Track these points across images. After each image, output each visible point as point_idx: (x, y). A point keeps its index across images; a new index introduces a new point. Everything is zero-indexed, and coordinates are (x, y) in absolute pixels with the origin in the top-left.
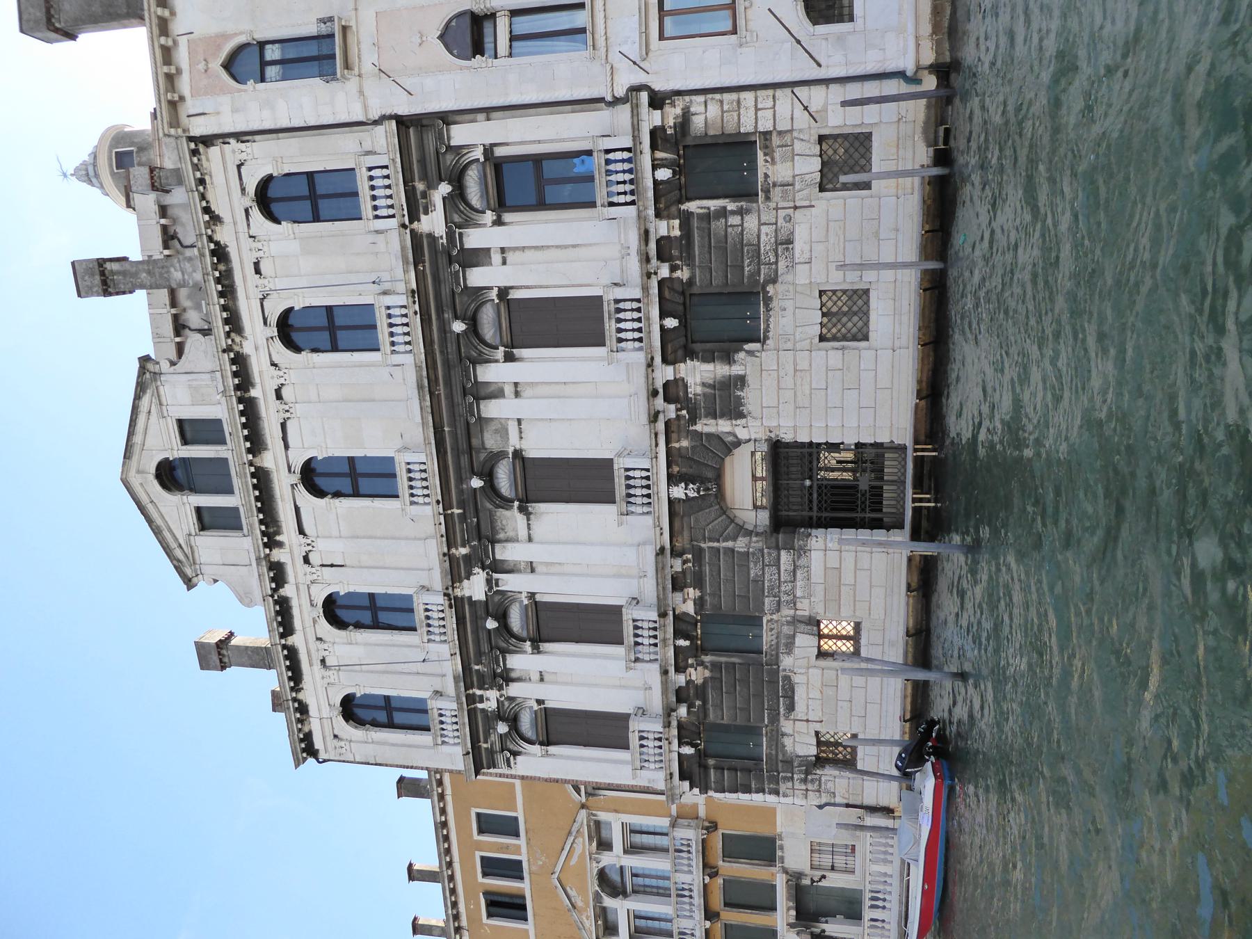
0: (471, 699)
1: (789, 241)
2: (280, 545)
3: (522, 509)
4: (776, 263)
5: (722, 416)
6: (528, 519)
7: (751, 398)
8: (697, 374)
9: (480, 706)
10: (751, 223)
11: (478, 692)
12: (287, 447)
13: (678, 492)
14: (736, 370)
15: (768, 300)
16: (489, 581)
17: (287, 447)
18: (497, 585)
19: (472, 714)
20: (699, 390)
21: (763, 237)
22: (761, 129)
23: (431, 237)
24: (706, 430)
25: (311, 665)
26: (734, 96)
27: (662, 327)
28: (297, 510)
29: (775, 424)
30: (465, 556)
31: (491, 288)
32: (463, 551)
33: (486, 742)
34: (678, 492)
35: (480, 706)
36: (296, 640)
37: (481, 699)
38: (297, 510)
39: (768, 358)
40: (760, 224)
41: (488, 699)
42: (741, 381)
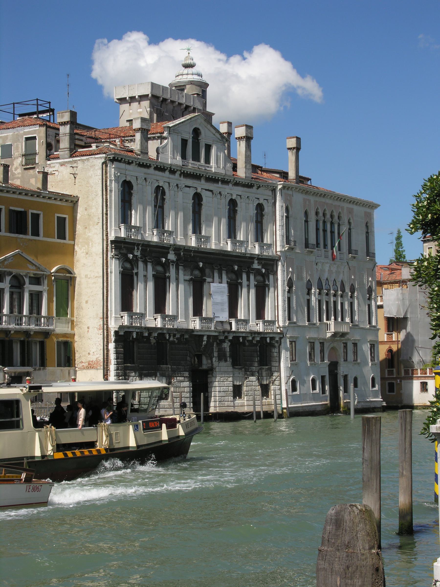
0: (138, 245)
1: (253, 375)
2: (180, 175)
3: (191, 279)
4: (249, 371)
5: (218, 354)
6: (188, 281)
7: (223, 363)
8: (226, 346)
9: (136, 248)
10: (256, 364)
11: (140, 249)
12: (206, 190)
13: (205, 338)
14: (228, 359)
15: (241, 369)
16: (173, 262)
17: (206, 190)
18: (172, 265)
19: (134, 244)
20: (223, 346)
21: (254, 368)
22: (272, 367)
23: (253, 263)
24: (214, 348)
25: (145, 173)
26: (278, 360)
27: (240, 336)
28: (189, 187)
29: (217, 370)
30: (180, 253)
31: (242, 280)
32: (182, 254)
33: (124, 247)
34: (205, 338)
35: (136, 248)
36: (151, 170)
37: (138, 249)
38: (189, 187)
39: (230, 369)
40: (256, 367)
41: (137, 252)
42: (226, 361)
